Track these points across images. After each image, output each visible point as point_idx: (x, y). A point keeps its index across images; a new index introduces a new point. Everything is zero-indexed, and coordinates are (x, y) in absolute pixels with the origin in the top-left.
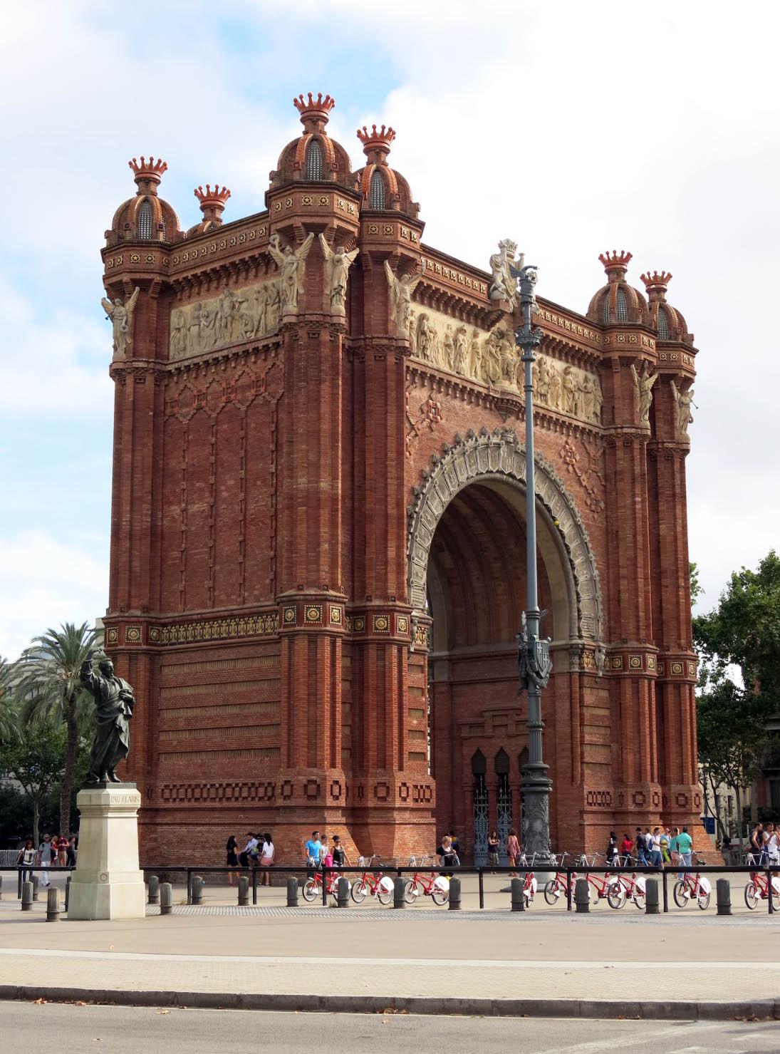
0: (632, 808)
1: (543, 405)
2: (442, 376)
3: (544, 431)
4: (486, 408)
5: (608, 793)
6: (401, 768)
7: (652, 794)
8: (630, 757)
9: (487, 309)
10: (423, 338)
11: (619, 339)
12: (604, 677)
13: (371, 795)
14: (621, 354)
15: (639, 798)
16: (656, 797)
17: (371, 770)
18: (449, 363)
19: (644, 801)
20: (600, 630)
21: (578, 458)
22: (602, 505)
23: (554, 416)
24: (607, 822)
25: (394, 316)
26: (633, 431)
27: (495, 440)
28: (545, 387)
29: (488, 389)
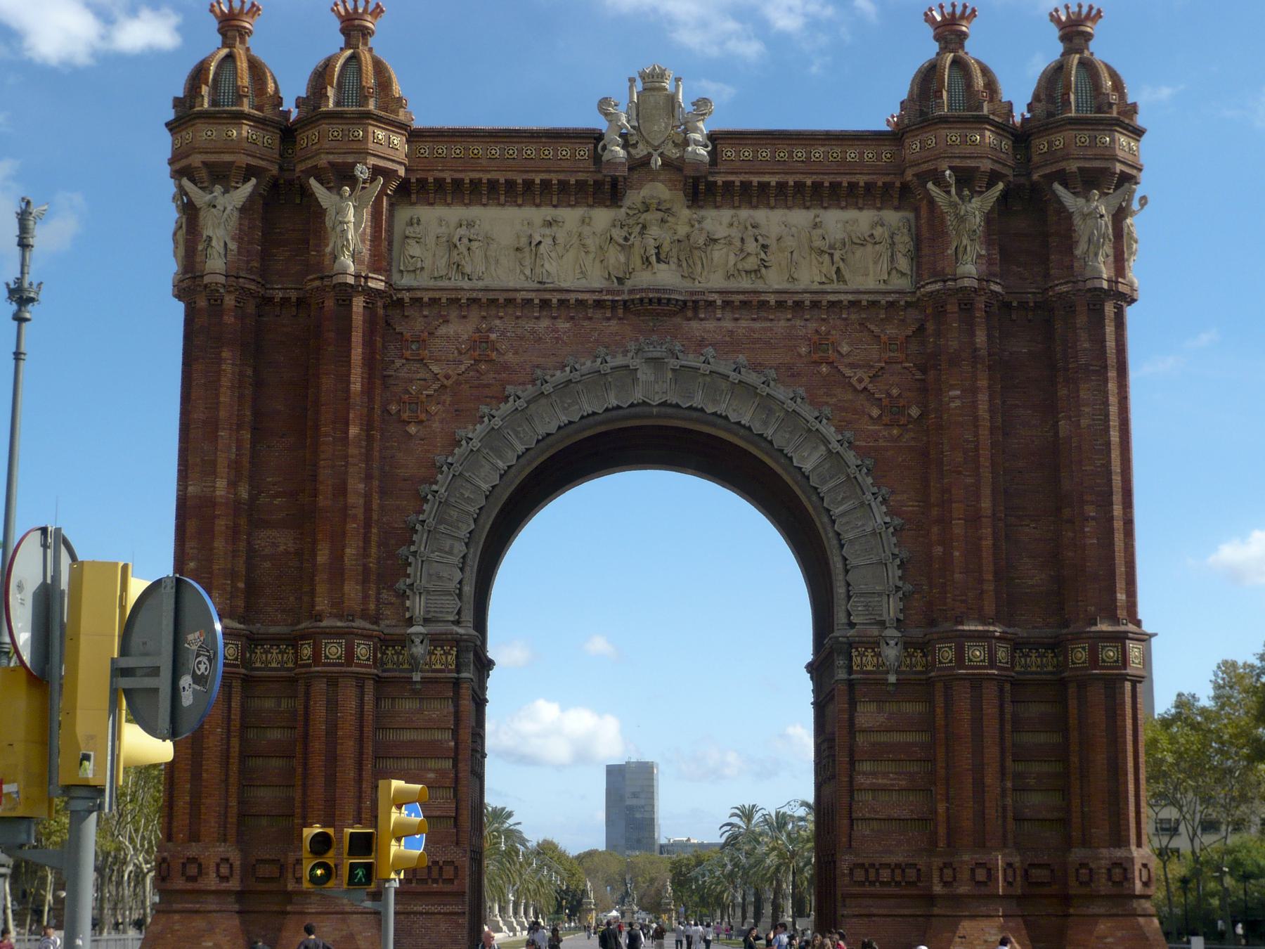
0: (938, 889)
1: (760, 286)
2: (491, 296)
3: (757, 325)
4: (609, 319)
8: (941, 807)
10: (455, 252)
11: (914, 146)
12: (899, 683)
14: (916, 170)
15: (948, 872)
16: (1010, 872)
20: (891, 609)
21: (845, 349)
22: (914, 412)
23: (772, 299)
24: (906, 912)
25: (331, 245)
26: (938, 286)
27: (620, 360)
29: (601, 292)
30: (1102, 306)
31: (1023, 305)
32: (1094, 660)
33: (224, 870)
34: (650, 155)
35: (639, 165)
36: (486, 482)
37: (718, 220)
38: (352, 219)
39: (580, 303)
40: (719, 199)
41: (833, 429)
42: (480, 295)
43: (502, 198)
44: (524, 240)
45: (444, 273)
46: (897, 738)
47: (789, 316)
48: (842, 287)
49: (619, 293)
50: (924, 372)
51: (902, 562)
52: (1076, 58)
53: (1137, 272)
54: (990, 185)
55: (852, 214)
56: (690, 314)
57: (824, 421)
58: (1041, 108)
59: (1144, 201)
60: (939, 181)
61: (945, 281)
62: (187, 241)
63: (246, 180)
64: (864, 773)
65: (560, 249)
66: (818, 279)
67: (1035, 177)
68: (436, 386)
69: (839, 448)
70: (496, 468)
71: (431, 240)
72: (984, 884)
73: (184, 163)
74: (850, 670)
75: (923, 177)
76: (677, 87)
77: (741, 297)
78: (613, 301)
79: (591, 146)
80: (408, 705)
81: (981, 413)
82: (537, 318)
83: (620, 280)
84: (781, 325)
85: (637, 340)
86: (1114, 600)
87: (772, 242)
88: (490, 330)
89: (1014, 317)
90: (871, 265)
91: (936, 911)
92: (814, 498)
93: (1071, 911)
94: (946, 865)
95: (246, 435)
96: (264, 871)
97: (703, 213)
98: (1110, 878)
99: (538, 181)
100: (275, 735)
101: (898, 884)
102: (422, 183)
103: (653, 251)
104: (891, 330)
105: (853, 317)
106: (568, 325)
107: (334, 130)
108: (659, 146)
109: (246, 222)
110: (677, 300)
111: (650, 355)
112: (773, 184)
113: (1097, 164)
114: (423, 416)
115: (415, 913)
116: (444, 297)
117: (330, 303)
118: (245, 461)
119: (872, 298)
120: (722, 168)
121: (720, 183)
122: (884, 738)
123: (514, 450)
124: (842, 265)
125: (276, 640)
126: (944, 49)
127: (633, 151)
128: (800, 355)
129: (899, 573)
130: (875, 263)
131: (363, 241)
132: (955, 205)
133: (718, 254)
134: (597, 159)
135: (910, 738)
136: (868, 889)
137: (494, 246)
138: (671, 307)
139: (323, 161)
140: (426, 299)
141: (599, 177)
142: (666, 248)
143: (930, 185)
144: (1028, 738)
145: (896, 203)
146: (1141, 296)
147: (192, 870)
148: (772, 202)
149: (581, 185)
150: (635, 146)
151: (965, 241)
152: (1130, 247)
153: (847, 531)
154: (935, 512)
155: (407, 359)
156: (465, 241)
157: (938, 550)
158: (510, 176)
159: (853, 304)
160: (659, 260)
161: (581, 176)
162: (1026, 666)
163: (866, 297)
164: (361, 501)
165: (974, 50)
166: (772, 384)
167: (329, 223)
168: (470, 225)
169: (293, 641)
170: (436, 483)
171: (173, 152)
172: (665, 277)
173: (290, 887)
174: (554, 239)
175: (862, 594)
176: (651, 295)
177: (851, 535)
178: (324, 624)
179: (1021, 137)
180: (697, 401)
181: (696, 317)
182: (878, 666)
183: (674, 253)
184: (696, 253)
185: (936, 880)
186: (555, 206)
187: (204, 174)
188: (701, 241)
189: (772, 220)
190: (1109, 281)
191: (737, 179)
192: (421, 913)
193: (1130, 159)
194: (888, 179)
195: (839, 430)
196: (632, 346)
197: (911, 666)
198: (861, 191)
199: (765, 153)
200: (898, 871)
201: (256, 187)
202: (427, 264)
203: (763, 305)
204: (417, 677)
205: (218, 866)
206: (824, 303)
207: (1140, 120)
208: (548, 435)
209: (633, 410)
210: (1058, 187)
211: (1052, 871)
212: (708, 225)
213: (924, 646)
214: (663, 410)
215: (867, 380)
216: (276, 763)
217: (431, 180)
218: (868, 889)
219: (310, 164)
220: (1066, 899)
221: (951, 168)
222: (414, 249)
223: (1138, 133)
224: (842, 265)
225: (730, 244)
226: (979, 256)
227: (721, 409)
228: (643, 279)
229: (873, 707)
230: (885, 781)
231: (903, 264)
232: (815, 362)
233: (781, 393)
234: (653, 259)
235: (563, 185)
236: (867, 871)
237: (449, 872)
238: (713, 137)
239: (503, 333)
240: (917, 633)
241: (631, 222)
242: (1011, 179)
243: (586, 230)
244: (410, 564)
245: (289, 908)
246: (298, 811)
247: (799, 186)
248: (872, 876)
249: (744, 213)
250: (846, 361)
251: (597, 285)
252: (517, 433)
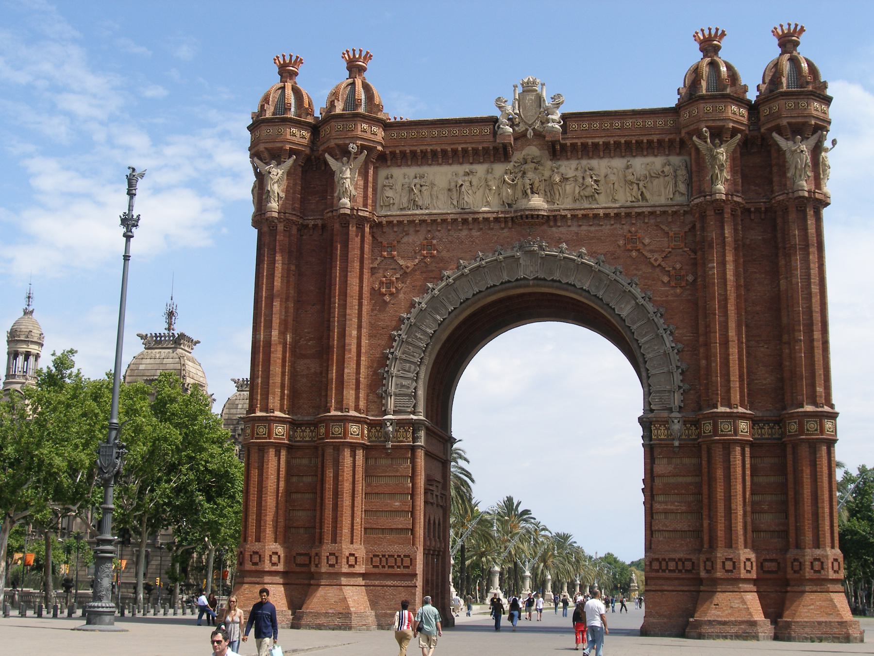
0: (703, 574)
2: (433, 218)
3: (593, 229)
4: (503, 229)
5: (690, 560)
6: (334, 540)
7: (743, 559)
8: (706, 523)
11: (685, 115)
12: (680, 447)
13: (267, 562)
14: (687, 130)
17: (317, 543)
18: (452, 203)
19: (712, 567)
20: (677, 400)
21: (647, 241)
22: (690, 278)
23: (601, 212)
26: (701, 199)
27: (509, 253)
28: (589, 189)
30: (805, 208)
31: (758, 210)
32: (801, 431)
33: (275, 559)
35: (520, 137)
36: (431, 329)
37: (569, 167)
38: (349, 176)
39: (486, 220)
40: (569, 154)
41: (639, 290)
42: (426, 218)
43: (440, 160)
44: (453, 184)
45: (405, 206)
46: (680, 479)
47: (612, 222)
48: (644, 204)
49: (508, 212)
50: (695, 253)
51: (682, 370)
52: (787, 56)
53: (830, 187)
54: (732, 137)
55: (650, 159)
56: (552, 223)
57: (634, 285)
58: (763, 88)
59: (834, 142)
60: (701, 136)
61: (705, 196)
62: (259, 194)
63: (290, 157)
64: (659, 502)
65: (474, 189)
66: (630, 199)
67: (762, 130)
68: (401, 273)
69: (643, 302)
70: (436, 320)
71: (398, 187)
72: (731, 571)
73: (256, 149)
74: (651, 439)
75: (690, 134)
76: (542, 89)
77: (582, 212)
79: (492, 127)
80: (384, 462)
81: (728, 277)
82: (461, 230)
83: (510, 205)
84: (607, 228)
85: (520, 240)
86: (814, 391)
87: (601, 178)
88: (433, 238)
89: (753, 217)
90: (663, 189)
91: (702, 588)
92: (629, 333)
93: (789, 589)
94: (708, 559)
95: (291, 305)
96: (300, 560)
97: (560, 163)
98: (812, 569)
99: (460, 149)
100: (308, 480)
101: (680, 571)
103: (528, 187)
104: (675, 229)
105: (652, 221)
106: (478, 233)
107: (339, 125)
108: (532, 124)
109: (292, 181)
111: (527, 249)
112: (601, 143)
113: (800, 120)
115: (387, 586)
116: (405, 220)
117: (337, 226)
118: (290, 320)
119: (663, 209)
120: (569, 135)
121: (569, 144)
122: (672, 480)
123: (447, 309)
124: (644, 190)
125: (308, 424)
126: (705, 56)
127: (517, 129)
128: (619, 246)
129: (681, 378)
130: (665, 188)
131: (356, 189)
132: (711, 150)
133: (569, 188)
134: (495, 134)
135: (689, 479)
136: (661, 574)
137: (436, 188)
138: (540, 220)
139: (332, 143)
140: (395, 222)
142: (536, 184)
143: (695, 138)
144: (762, 480)
146: (832, 200)
147: (256, 559)
148: (601, 154)
149: (486, 150)
150: (518, 125)
151: (717, 171)
152: (824, 171)
153: (649, 353)
154: (701, 339)
156: (418, 186)
157: (703, 362)
158: (443, 147)
159: (652, 213)
160: (532, 193)
161: (485, 145)
162: (762, 434)
163: (659, 209)
164: (355, 341)
165: (724, 55)
166: (602, 264)
167: (336, 180)
168: (422, 177)
169: (315, 424)
171: (252, 142)
172: (537, 202)
173: (313, 569)
174: (471, 183)
175: (659, 392)
176: (527, 213)
177: (650, 355)
178: (333, 413)
179: (753, 108)
180: (556, 277)
181: (556, 225)
182: (668, 435)
183: (542, 188)
184: (555, 187)
185: (702, 568)
186: (471, 163)
187: (266, 155)
188: (558, 180)
189: (601, 165)
190: (809, 192)
191: (579, 142)
192: (390, 586)
193: (821, 115)
194: (672, 136)
195: (643, 290)
196: (517, 244)
197: (689, 435)
198: (656, 144)
199: (597, 125)
200: (680, 563)
201: (295, 161)
202: (396, 201)
203: (596, 216)
204: (390, 445)
205: (271, 556)
206: (633, 213)
207: (829, 92)
208: (467, 299)
210: (774, 135)
211: (779, 563)
212: (563, 170)
213: (696, 423)
214: (535, 282)
215: (660, 260)
216: (307, 496)
217: (398, 152)
218: (661, 574)
219: (326, 146)
220: (787, 583)
221: (707, 127)
222: (389, 193)
223: (828, 100)
224: (644, 190)
225: (576, 180)
226: (727, 180)
228: (522, 204)
229: (665, 461)
230: (672, 507)
231: (682, 188)
232: (629, 250)
233: (607, 269)
234: (529, 191)
235: (475, 151)
236: (660, 563)
237: (407, 561)
238: (564, 117)
239: (441, 240)
240: (691, 416)
241: (517, 170)
242: (747, 132)
243: (490, 177)
244: (385, 378)
245: (312, 582)
246: (318, 525)
247: (617, 144)
248: (664, 567)
249: (584, 162)
250: (648, 248)
251: (495, 209)
252: (448, 298)
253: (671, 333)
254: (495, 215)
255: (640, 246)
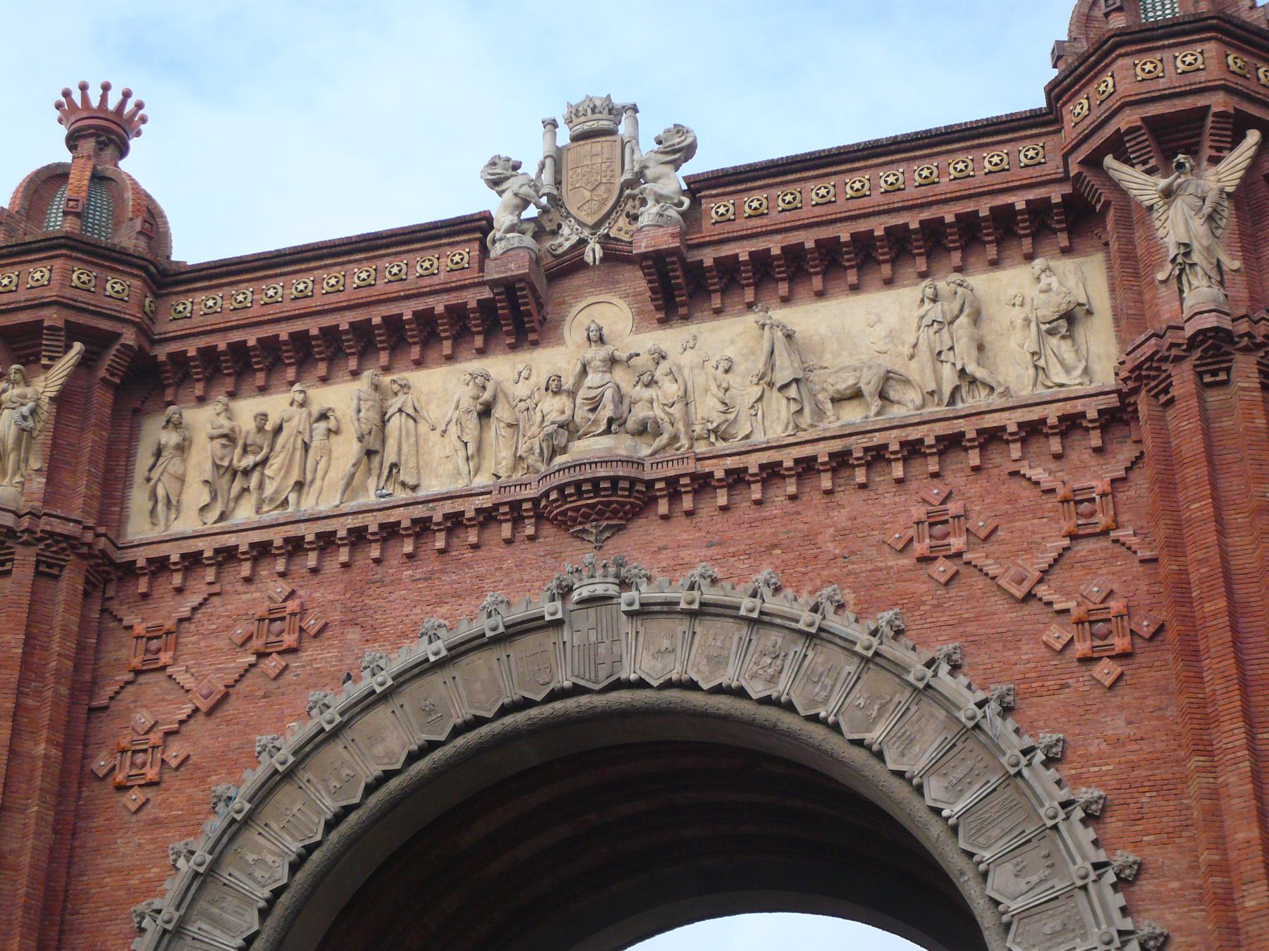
9: (471, 298)
14: (1082, 153)
34: (582, 242)
39: (455, 522)
75: (1093, 162)
78: (515, 505)
79: (476, 245)
102: (179, 359)
110: (633, 481)
111: (585, 592)
114: (151, 773)
121: (708, 262)
141: (486, 293)
145: (1063, 240)
149: (457, 313)
150: (555, 233)
155: (138, 672)
170: (162, 894)
191: (742, 251)
209: (559, 706)
227: (728, 677)
238: (698, 187)
253: (1090, 819)
254: (485, 502)
255: (957, 543)
